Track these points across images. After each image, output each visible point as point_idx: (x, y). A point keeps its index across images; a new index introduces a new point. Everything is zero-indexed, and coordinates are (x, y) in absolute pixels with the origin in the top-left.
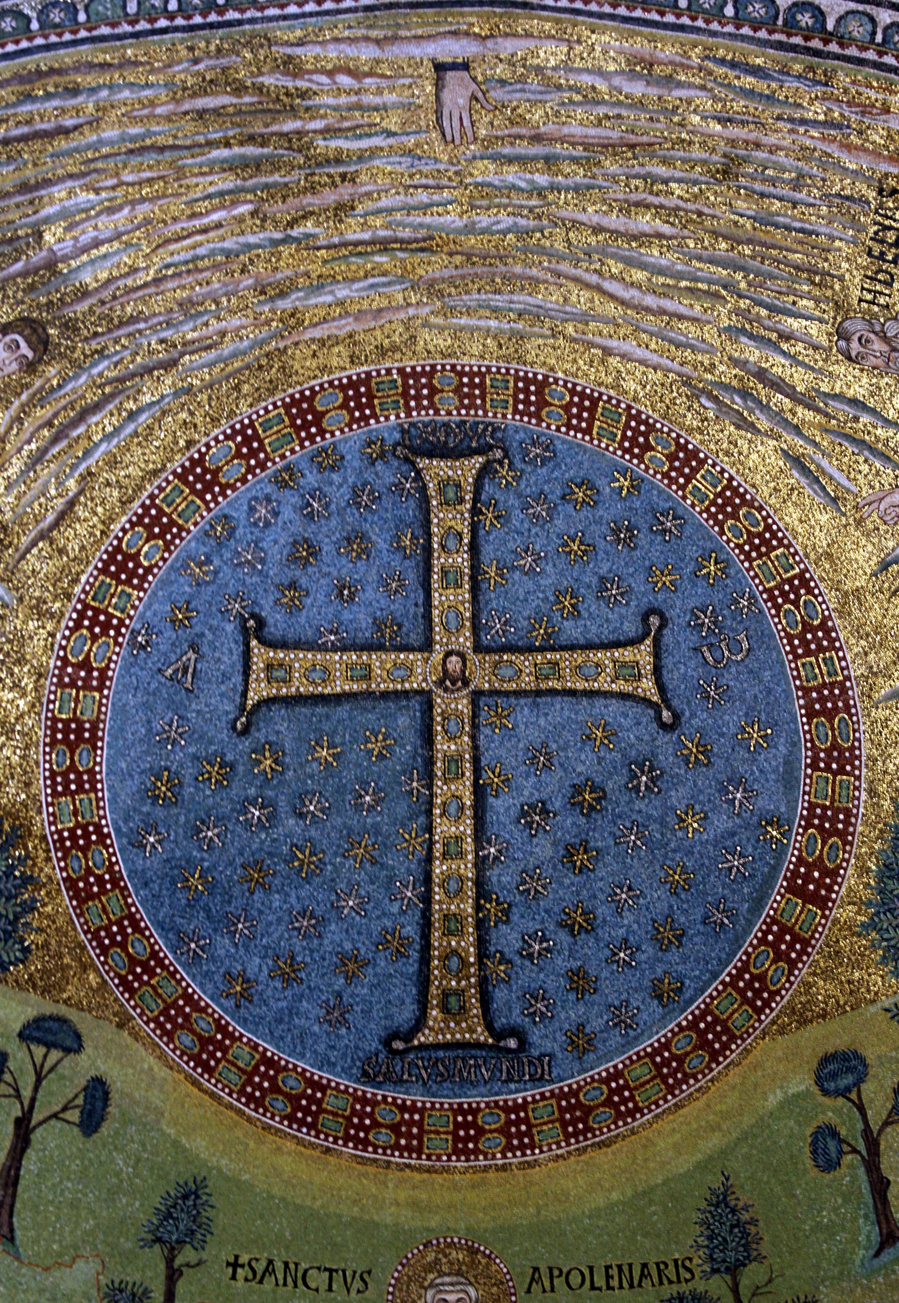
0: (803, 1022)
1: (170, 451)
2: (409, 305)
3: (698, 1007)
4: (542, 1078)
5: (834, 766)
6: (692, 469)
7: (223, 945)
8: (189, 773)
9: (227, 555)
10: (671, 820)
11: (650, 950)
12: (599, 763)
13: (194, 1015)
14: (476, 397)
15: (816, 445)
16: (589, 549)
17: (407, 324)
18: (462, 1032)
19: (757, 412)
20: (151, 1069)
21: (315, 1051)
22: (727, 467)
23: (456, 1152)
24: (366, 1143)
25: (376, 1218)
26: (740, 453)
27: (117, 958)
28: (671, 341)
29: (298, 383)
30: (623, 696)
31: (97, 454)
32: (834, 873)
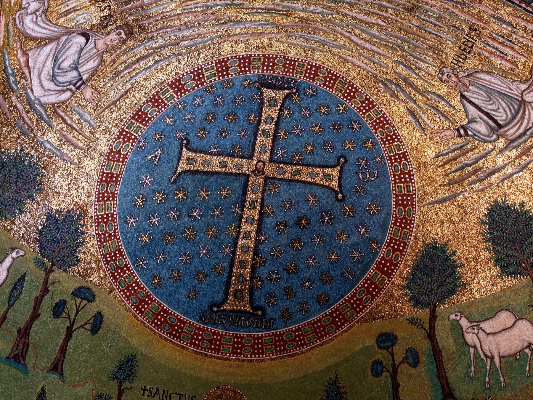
0: (374, 319)
27: (112, 266)
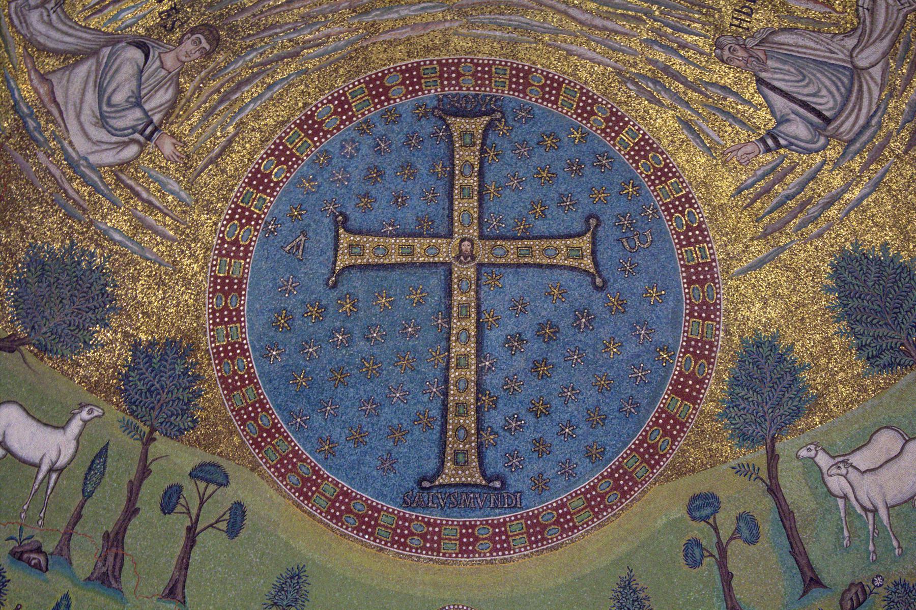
0: (680, 474)
1: (293, 110)
2: (446, 21)
3: (614, 464)
4: (515, 506)
5: (704, 315)
6: (620, 127)
7: (318, 420)
8: (298, 311)
9: (326, 176)
10: (600, 346)
11: (585, 428)
12: (555, 310)
13: (299, 464)
14: (486, 79)
15: (699, 114)
16: (553, 176)
17: (444, 32)
18: (466, 477)
19: (663, 93)
20: (271, 497)
21: (374, 487)
22: (642, 127)
23: (462, 552)
24: (405, 545)
25: (411, 592)
26: (651, 118)
27: (251, 427)
28: (610, 47)
29: (374, 68)
30: (572, 269)
31: (247, 112)
32: (701, 382)
